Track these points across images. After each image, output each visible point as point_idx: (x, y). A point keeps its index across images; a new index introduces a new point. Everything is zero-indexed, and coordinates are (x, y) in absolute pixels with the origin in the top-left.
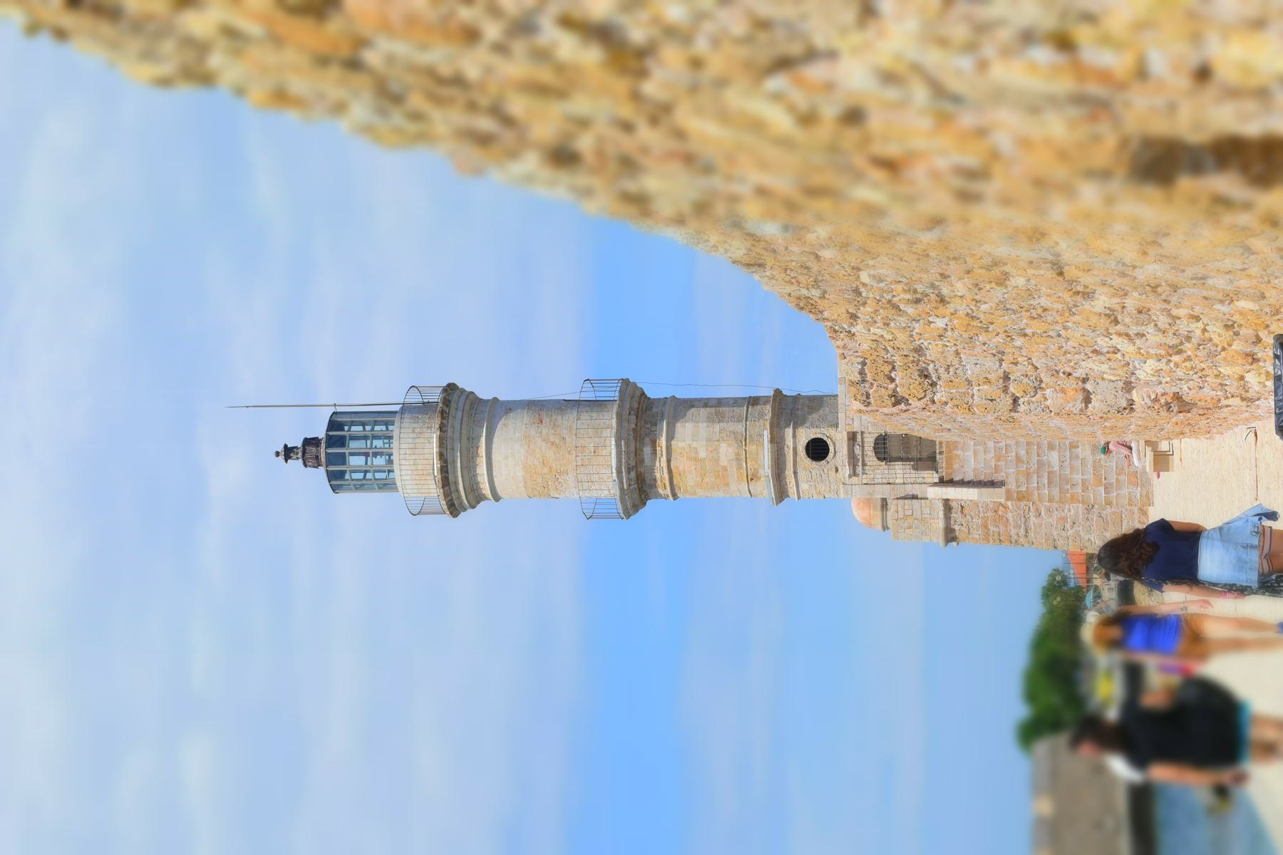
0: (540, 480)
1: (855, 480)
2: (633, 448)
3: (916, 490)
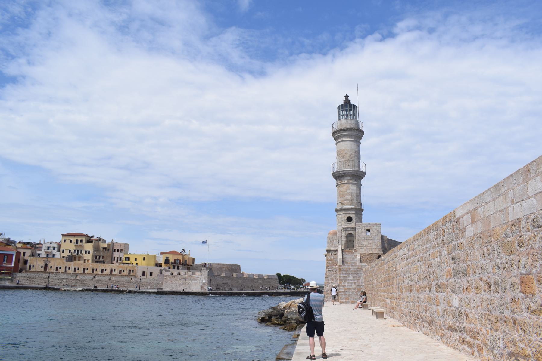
3: (340, 243)
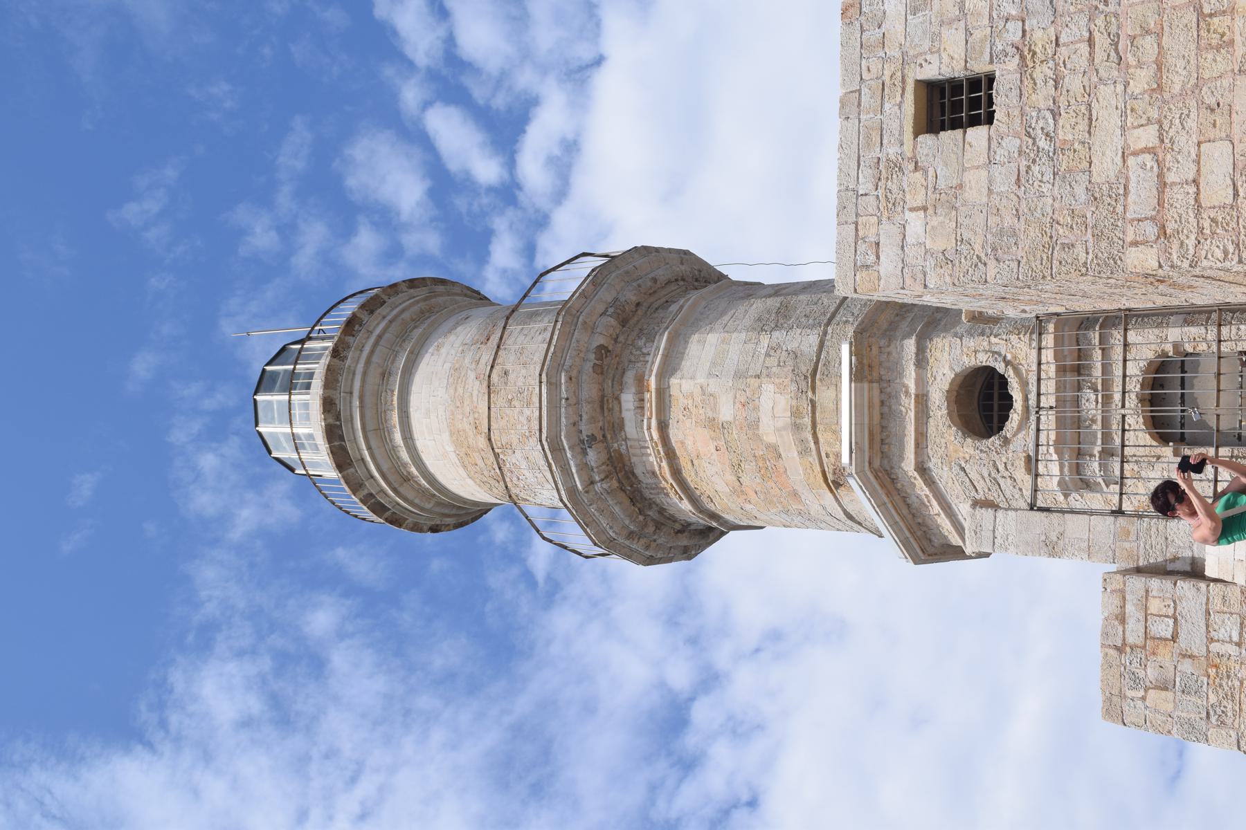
0: (480, 463)
1: (1076, 501)
2: (589, 390)
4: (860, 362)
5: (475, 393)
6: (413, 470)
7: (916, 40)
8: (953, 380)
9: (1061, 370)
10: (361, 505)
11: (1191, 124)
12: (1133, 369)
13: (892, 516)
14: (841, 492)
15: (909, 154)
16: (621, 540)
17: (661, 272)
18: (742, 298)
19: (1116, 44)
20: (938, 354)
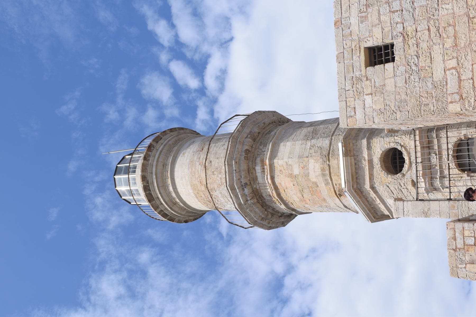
0: (203, 196)
1: (432, 196)
2: (244, 166)
4: (346, 149)
5: (199, 170)
6: (177, 200)
7: (363, 32)
8: (382, 154)
9: (422, 148)
10: (158, 215)
11: (469, 57)
12: (450, 146)
13: (362, 205)
14: (342, 198)
15: (364, 75)
16: (259, 221)
17: (266, 120)
18: (298, 128)
19: (439, 30)
20: (375, 144)
